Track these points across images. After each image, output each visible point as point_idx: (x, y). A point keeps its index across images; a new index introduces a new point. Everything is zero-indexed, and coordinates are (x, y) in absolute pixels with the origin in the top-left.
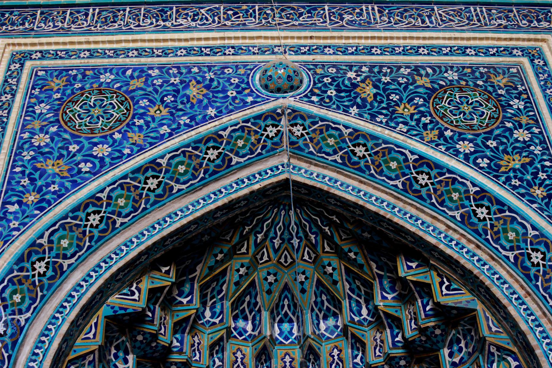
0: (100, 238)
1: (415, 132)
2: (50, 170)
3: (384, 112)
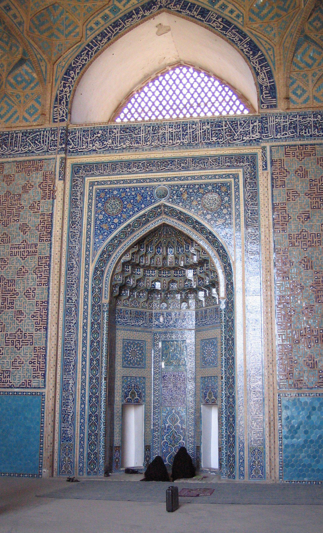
0: (118, 245)
1: (196, 212)
2: (104, 228)
3: (189, 204)
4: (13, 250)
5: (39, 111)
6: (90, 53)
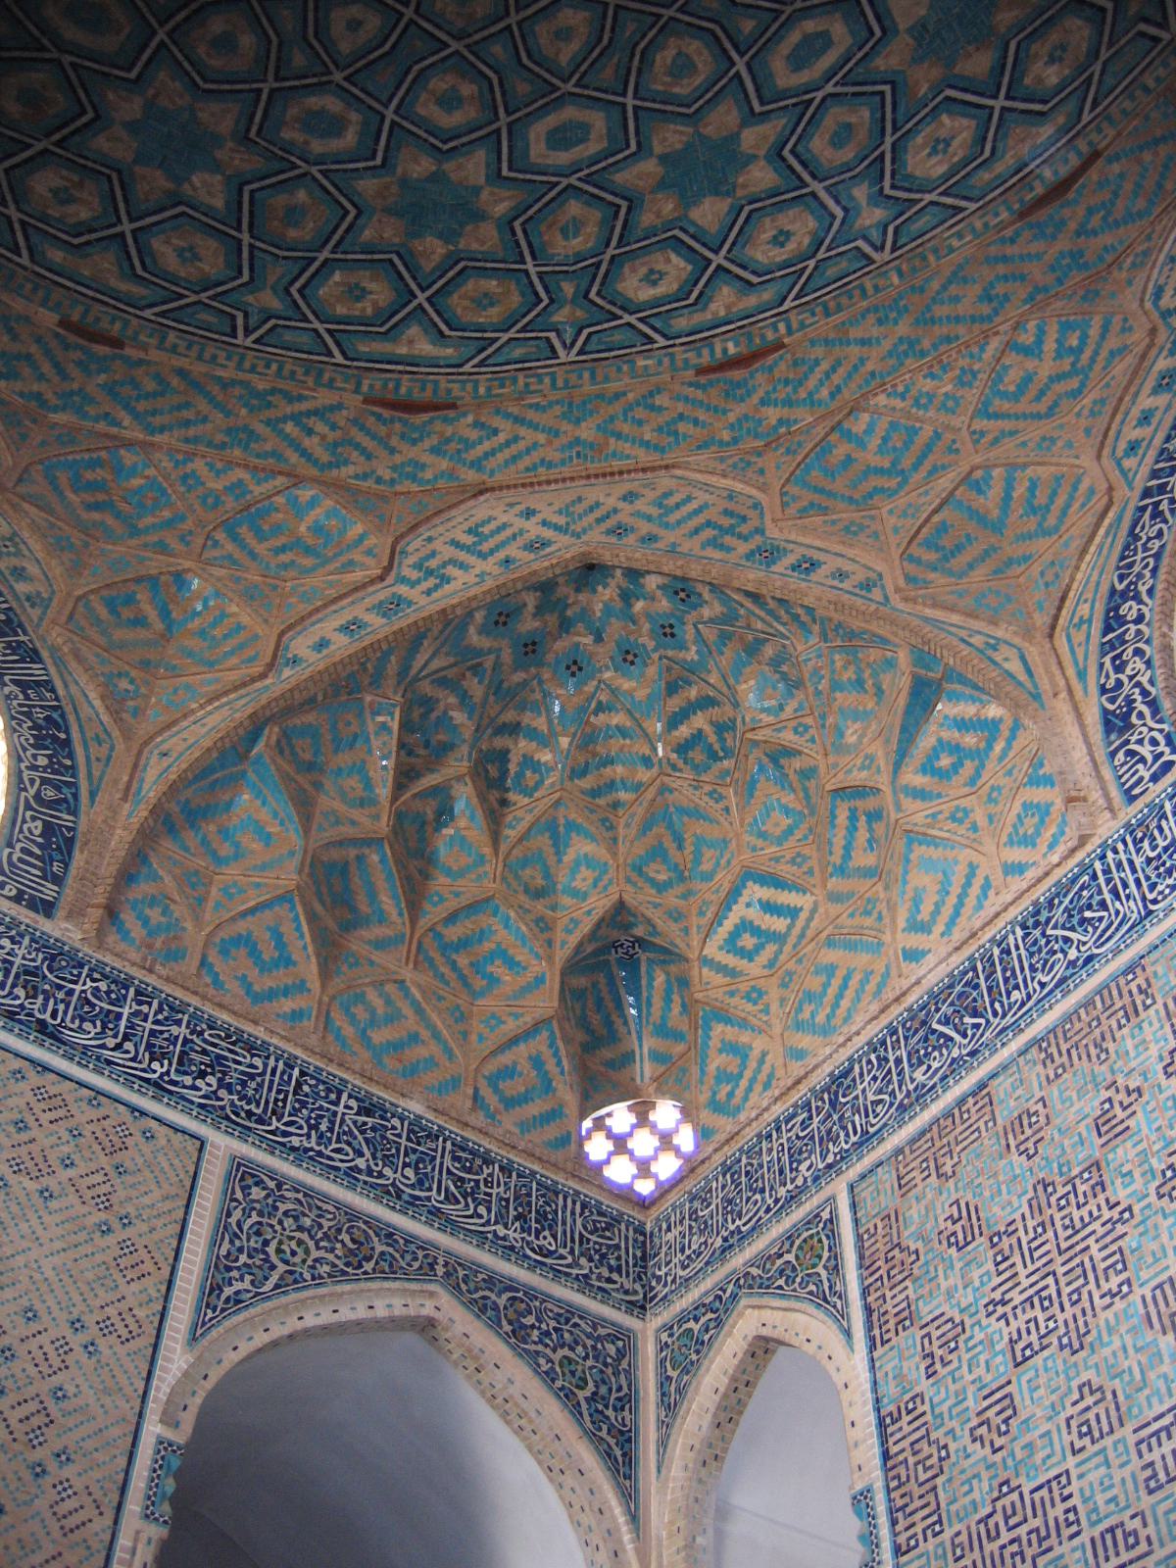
4: (1155, 1456)
5: (1059, 803)
6: (1164, 506)
